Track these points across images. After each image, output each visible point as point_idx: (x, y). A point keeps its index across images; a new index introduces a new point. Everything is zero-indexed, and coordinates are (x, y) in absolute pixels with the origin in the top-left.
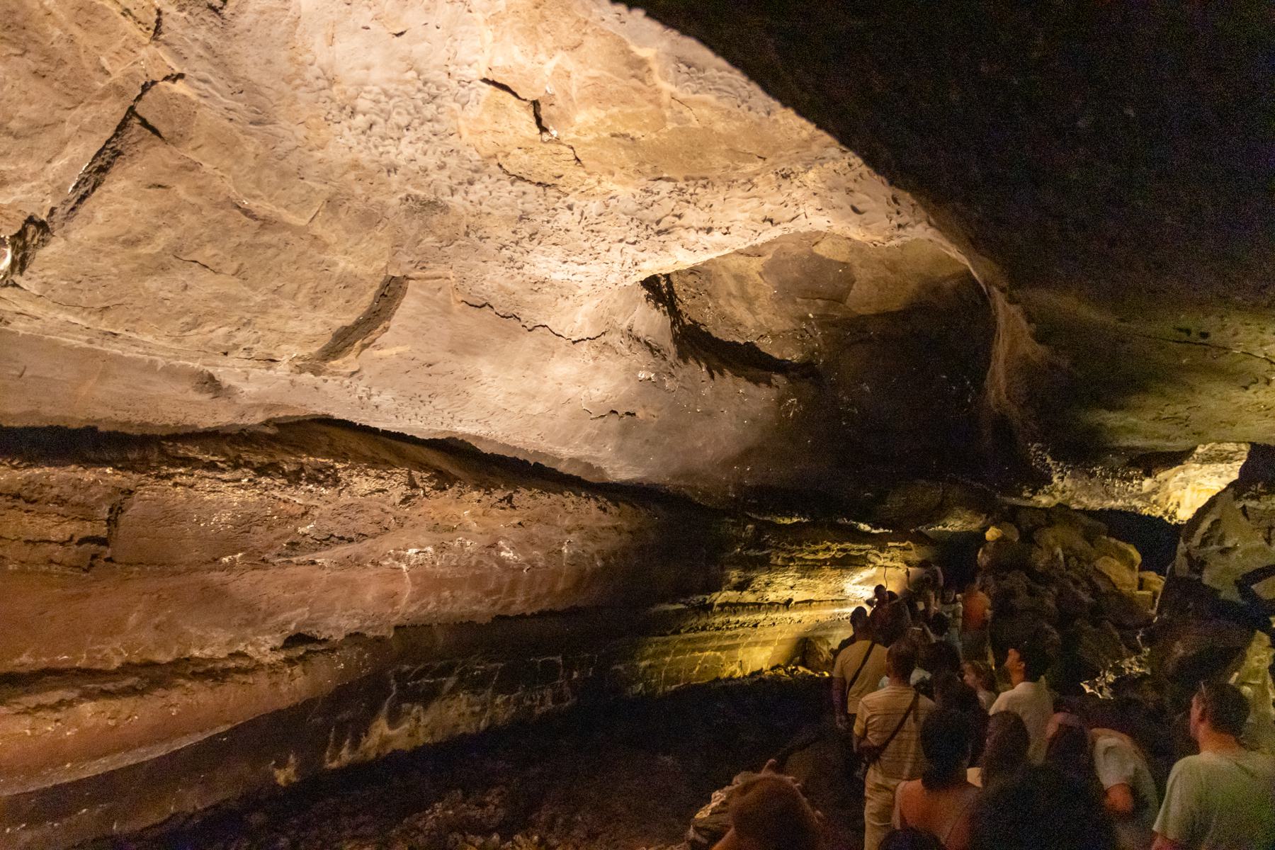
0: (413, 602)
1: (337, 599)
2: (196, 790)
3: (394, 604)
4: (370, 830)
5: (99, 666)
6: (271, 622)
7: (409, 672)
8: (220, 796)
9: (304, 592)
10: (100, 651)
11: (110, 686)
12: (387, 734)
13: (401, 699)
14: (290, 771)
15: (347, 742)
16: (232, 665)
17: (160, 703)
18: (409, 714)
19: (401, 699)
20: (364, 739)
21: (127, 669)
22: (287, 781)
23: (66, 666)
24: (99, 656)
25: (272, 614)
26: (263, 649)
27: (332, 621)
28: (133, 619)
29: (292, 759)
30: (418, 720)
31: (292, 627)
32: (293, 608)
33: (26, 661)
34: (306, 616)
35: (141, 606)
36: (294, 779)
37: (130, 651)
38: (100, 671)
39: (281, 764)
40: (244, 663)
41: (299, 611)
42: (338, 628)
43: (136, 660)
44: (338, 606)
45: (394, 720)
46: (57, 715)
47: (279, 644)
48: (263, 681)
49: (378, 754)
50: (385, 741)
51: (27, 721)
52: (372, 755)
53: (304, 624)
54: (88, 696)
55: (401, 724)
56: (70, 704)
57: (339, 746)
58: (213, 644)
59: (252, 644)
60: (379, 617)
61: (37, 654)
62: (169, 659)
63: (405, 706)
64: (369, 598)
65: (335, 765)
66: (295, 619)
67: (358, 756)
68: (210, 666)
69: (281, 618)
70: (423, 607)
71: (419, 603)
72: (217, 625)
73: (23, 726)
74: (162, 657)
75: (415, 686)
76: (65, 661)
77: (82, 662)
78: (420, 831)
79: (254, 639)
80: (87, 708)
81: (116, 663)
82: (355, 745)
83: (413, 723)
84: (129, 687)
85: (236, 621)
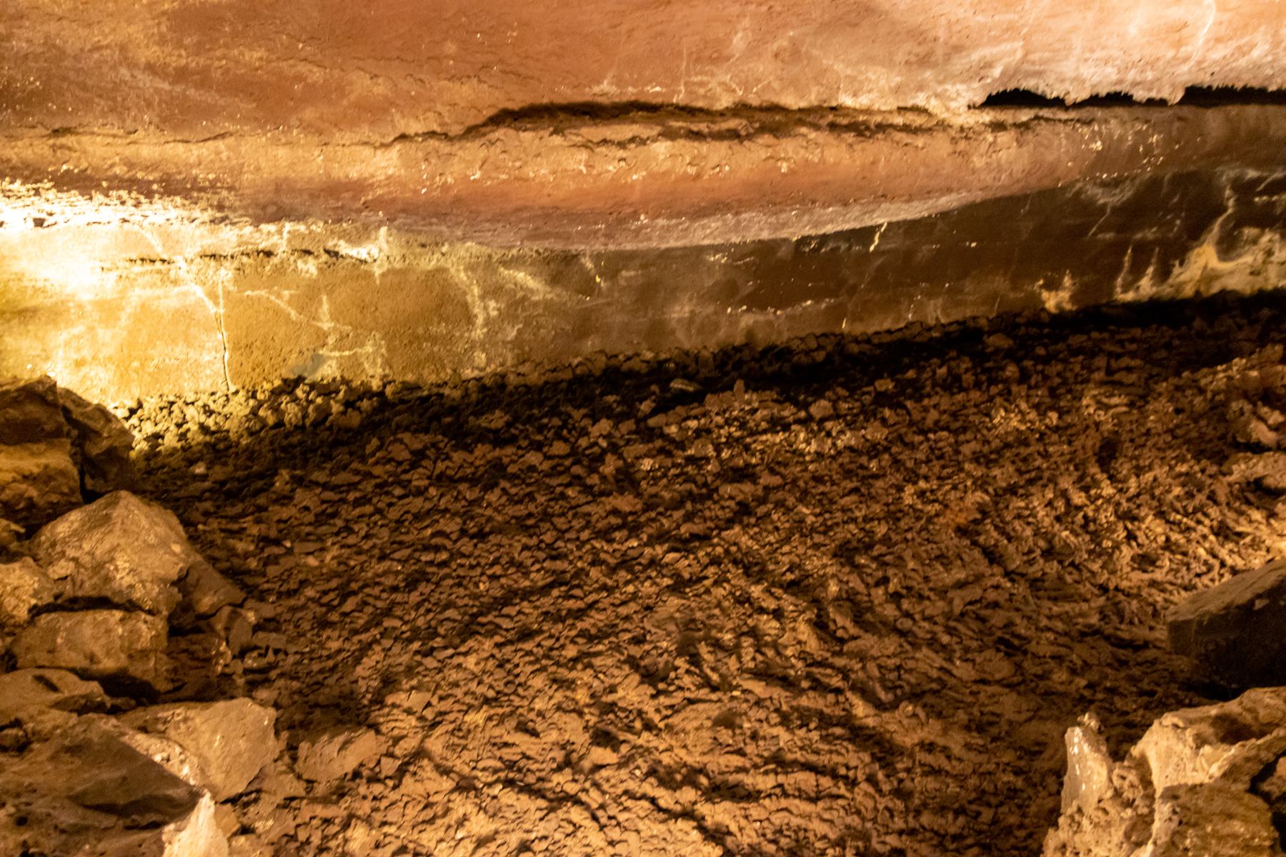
0: (1218, 40)
1: (1073, 30)
2: (940, 301)
3: (1179, 44)
4: (1133, 378)
5: (700, 104)
6: (959, 63)
7: (1258, 181)
8: (969, 312)
9: (1011, 16)
10: (702, 84)
11: (703, 127)
12: (1206, 266)
13: (1241, 221)
14: (1064, 295)
15: (1150, 270)
16: (899, 120)
17: (764, 154)
18: (1255, 241)
19: (1241, 221)
20: (1176, 270)
21: (741, 109)
22: (1058, 306)
23: (659, 100)
24: (702, 91)
25: (958, 49)
26: (953, 105)
27: (1068, 67)
28: (739, 42)
29: (1067, 281)
30: (1269, 253)
31: (997, 72)
32: (996, 40)
33: (606, 90)
34: (1019, 55)
35: (746, 22)
36: (1068, 307)
37: (746, 86)
38: (701, 110)
39: (1052, 285)
40: (918, 120)
41: (1006, 47)
42: (1078, 80)
43: (754, 101)
44: (1077, 42)
45: (1228, 247)
46: (621, 153)
47: (980, 98)
48: (940, 146)
49: (1198, 293)
50: (1210, 276)
51: (583, 155)
52: (1189, 291)
53: (1015, 72)
54: (670, 135)
55: (1239, 256)
56: (643, 142)
57: (1137, 271)
58: (872, 91)
59: (937, 96)
60: (1152, 64)
61: (619, 82)
62: (803, 104)
63: (1249, 232)
64: (1133, 30)
65: (1130, 296)
66: (1003, 61)
67: (1166, 290)
68: (861, 118)
69: (976, 56)
70: (1242, 51)
71: (1233, 45)
72: (871, 60)
73: (577, 161)
74: (791, 101)
75: (1271, 205)
76: (657, 94)
77: (680, 98)
78: (1202, 391)
79: (939, 89)
80: (662, 148)
81: (725, 102)
82: (1164, 274)
83: (1260, 257)
84: (728, 130)
85: (900, 57)
